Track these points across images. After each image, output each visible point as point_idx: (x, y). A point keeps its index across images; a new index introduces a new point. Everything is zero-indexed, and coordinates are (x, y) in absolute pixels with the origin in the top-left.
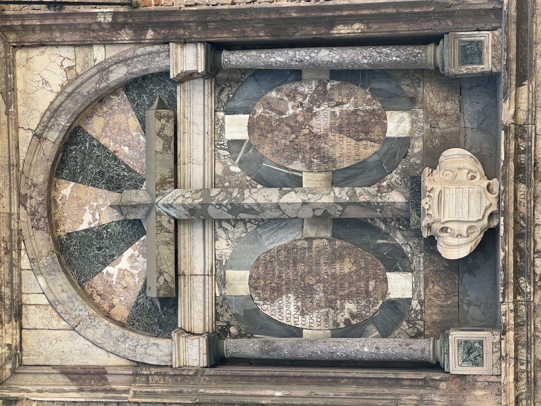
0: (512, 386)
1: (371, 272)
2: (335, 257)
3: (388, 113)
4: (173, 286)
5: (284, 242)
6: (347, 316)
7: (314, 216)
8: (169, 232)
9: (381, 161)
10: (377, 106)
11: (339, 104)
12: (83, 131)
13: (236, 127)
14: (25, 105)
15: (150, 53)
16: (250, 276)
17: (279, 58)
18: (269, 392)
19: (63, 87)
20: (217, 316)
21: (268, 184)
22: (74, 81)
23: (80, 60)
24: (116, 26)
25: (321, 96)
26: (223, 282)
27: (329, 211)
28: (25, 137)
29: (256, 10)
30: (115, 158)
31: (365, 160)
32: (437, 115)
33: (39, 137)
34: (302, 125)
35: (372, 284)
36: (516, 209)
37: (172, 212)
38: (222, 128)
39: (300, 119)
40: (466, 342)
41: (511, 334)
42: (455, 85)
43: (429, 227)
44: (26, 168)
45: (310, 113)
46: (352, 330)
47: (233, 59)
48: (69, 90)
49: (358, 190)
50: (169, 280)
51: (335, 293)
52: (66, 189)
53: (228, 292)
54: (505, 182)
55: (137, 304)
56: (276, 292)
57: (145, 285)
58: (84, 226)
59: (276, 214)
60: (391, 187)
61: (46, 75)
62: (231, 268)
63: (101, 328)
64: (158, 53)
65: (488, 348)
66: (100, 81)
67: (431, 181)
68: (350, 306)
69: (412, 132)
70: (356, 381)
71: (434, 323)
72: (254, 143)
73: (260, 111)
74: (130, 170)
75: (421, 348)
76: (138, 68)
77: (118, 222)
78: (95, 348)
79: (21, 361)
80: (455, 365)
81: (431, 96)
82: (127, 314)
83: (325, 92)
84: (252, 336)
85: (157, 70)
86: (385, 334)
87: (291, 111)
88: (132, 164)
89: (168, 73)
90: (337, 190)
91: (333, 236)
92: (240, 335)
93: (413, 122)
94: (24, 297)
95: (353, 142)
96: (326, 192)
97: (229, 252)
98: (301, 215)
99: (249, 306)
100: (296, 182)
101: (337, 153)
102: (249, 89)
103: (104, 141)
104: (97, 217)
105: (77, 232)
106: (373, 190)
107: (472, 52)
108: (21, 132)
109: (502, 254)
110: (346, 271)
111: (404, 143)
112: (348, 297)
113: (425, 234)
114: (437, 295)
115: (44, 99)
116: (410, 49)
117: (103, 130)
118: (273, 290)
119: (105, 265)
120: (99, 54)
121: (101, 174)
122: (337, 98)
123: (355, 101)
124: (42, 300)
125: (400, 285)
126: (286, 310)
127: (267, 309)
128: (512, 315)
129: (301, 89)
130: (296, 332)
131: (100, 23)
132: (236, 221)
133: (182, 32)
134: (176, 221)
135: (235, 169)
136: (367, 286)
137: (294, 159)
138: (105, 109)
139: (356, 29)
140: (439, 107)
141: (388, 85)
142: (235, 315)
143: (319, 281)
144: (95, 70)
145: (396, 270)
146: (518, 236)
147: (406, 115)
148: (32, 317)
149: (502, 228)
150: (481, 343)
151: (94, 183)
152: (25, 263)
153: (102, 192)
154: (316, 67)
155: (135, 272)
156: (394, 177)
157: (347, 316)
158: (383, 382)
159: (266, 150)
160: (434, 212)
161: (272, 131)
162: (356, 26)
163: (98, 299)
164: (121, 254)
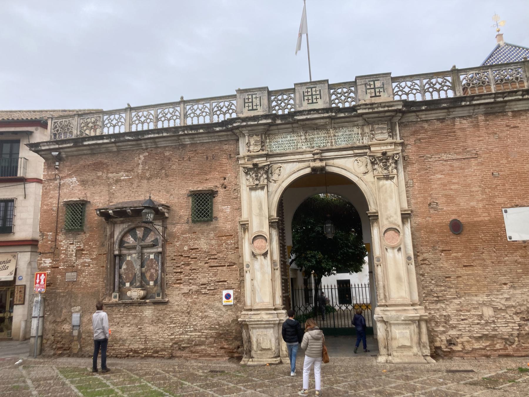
13: (152, 256)
26: (129, 256)
45: (153, 269)
46: (120, 276)
47: (160, 256)
52: (143, 229)
56: (127, 264)
75: (116, 289)
80: (114, 294)
111: (149, 284)
125: (128, 285)
126: (124, 266)
127: (124, 263)
130: (120, 268)
151: (144, 233)
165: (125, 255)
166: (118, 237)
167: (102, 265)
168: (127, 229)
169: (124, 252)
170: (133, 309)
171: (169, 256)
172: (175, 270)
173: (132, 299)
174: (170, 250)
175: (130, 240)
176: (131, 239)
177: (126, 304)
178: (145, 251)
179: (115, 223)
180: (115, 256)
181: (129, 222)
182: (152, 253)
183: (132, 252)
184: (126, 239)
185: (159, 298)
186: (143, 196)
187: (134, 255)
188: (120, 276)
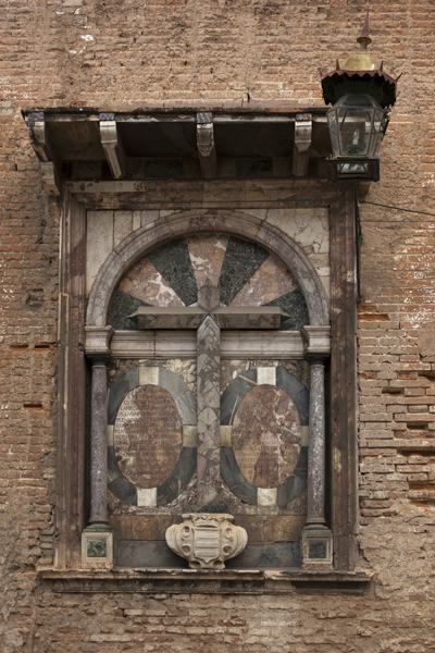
0: (74, 576)
1: (157, 476)
2: (168, 450)
3: (275, 489)
4: (146, 327)
5: (180, 412)
6: (124, 458)
7: (198, 434)
8: (188, 324)
9: (240, 484)
10: (281, 481)
11: (282, 452)
12: (266, 258)
13: (267, 375)
14: (285, 214)
15: (323, 310)
16: (153, 386)
17: (318, 408)
18: (66, 400)
19: (298, 244)
20: (124, 360)
21: (222, 399)
22: (305, 251)
23: (318, 256)
24: (344, 285)
25: (289, 440)
26: (149, 366)
27: (202, 445)
28: (261, 214)
29: (354, 391)
30: (244, 283)
31: (239, 471)
32: (273, 524)
33: (261, 224)
34: (267, 425)
35: (148, 477)
36: (203, 581)
37: (202, 327)
38: (266, 365)
39: (272, 424)
40: (105, 545)
41: (111, 577)
42: (294, 541)
43: (190, 518)
44: (237, 214)
45: (276, 431)
46: (113, 461)
47: (318, 375)
48: (297, 248)
49: (218, 467)
50: (151, 324)
51: (141, 449)
53: (142, 369)
54: (221, 574)
55: (133, 298)
56: (141, 405)
57: (147, 305)
58: (193, 258)
59: (200, 406)
60: (220, 491)
61: (307, 230)
62: (160, 371)
63: (115, 271)
64: (323, 316)
65: (101, 560)
66: (302, 271)
67: (221, 522)
68: (131, 460)
69: (262, 507)
70: (75, 465)
71: (119, 522)
72: (254, 390)
73: (278, 393)
74: (235, 294)
75: (99, 513)
76: (311, 301)
77: (196, 285)
78: (99, 266)
79: (90, 210)
80: (88, 537)
81: (288, 521)
82: (126, 291)
83: (291, 443)
84: (108, 386)
85: (310, 315)
86: (110, 486)
87: (278, 417)
88: (240, 295)
89: (308, 324)
90: (218, 451)
91: (185, 448)
92: (109, 378)
93: (268, 507)
94: (138, 212)
95: (254, 463)
96: (217, 442)
97: (173, 370)
98: (200, 424)
99: (132, 385)
100: (224, 420)
101: (246, 451)
102: (295, 386)
103: (257, 273)
104: (200, 268)
105: (188, 253)
106: (218, 477)
107: (318, 550)
108: (265, 211)
109: (169, 570)
110: (158, 458)
111: (254, 501)
112: (138, 459)
113: (184, 516)
114: (139, 524)
115: (290, 229)
116: (322, 505)
117: (266, 273)
118: (144, 403)
119: (162, 274)
120: (324, 272)
121: (232, 272)
122: (287, 451)
123: (285, 464)
124: (136, 226)
125: (147, 497)
126: (128, 413)
127: (129, 398)
128: (125, 577)
129: (294, 424)
130: (111, 419)
131: (346, 273)
132: (196, 375)
133: (339, 334)
134: (196, 330)
135: (235, 374)
136: (146, 473)
137: (242, 419)
138: (282, 275)
139: (338, 466)
140: (279, 526)
141: (293, 489)
142: (125, 374)
143: (150, 437)
144: (310, 267)
145: (158, 494)
146: (182, 583)
147: (274, 502)
148: (122, 219)
149: (188, 571)
150: (104, 556)
151: (226, 266)
152: (164, 213)
153: (219, 273)
154: (311, 436)
155: (157, 297)
156: (228, 494)
157: (124, 458)
158: (74, 485)
159: (249, 398)
160: (200, 522)
161: (263, 403)
162: (340, 466)
163: (137, 268)
164: (171, 286)
165: (133, 360)
166: (103, 270)
167: (29, 398)
168: (148, 240)
169: (128, 346)
170: (194, 607)
171: (373, 374)
172: (399, 442)
173: (184, 563)
174: (377, 349)
175: (158, 293)
176: (164, 289)
177: (157, 582)
178: (234, 346)
179: (92, 206)
180: (91, 360)
181: (163, 205)
182: (266, 360)
183: (165, 347)
184: (134, 287)
185: (326, 564)
186: (237, 84)
187: (178, 364)
188: (113, 461)
